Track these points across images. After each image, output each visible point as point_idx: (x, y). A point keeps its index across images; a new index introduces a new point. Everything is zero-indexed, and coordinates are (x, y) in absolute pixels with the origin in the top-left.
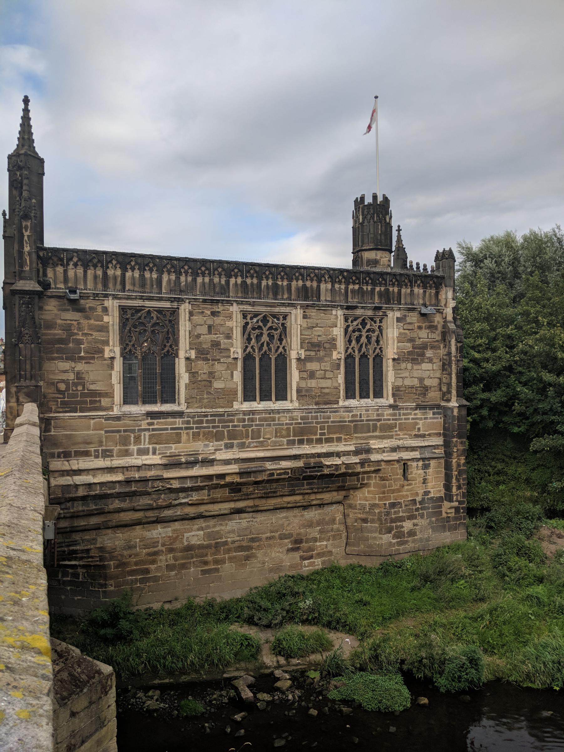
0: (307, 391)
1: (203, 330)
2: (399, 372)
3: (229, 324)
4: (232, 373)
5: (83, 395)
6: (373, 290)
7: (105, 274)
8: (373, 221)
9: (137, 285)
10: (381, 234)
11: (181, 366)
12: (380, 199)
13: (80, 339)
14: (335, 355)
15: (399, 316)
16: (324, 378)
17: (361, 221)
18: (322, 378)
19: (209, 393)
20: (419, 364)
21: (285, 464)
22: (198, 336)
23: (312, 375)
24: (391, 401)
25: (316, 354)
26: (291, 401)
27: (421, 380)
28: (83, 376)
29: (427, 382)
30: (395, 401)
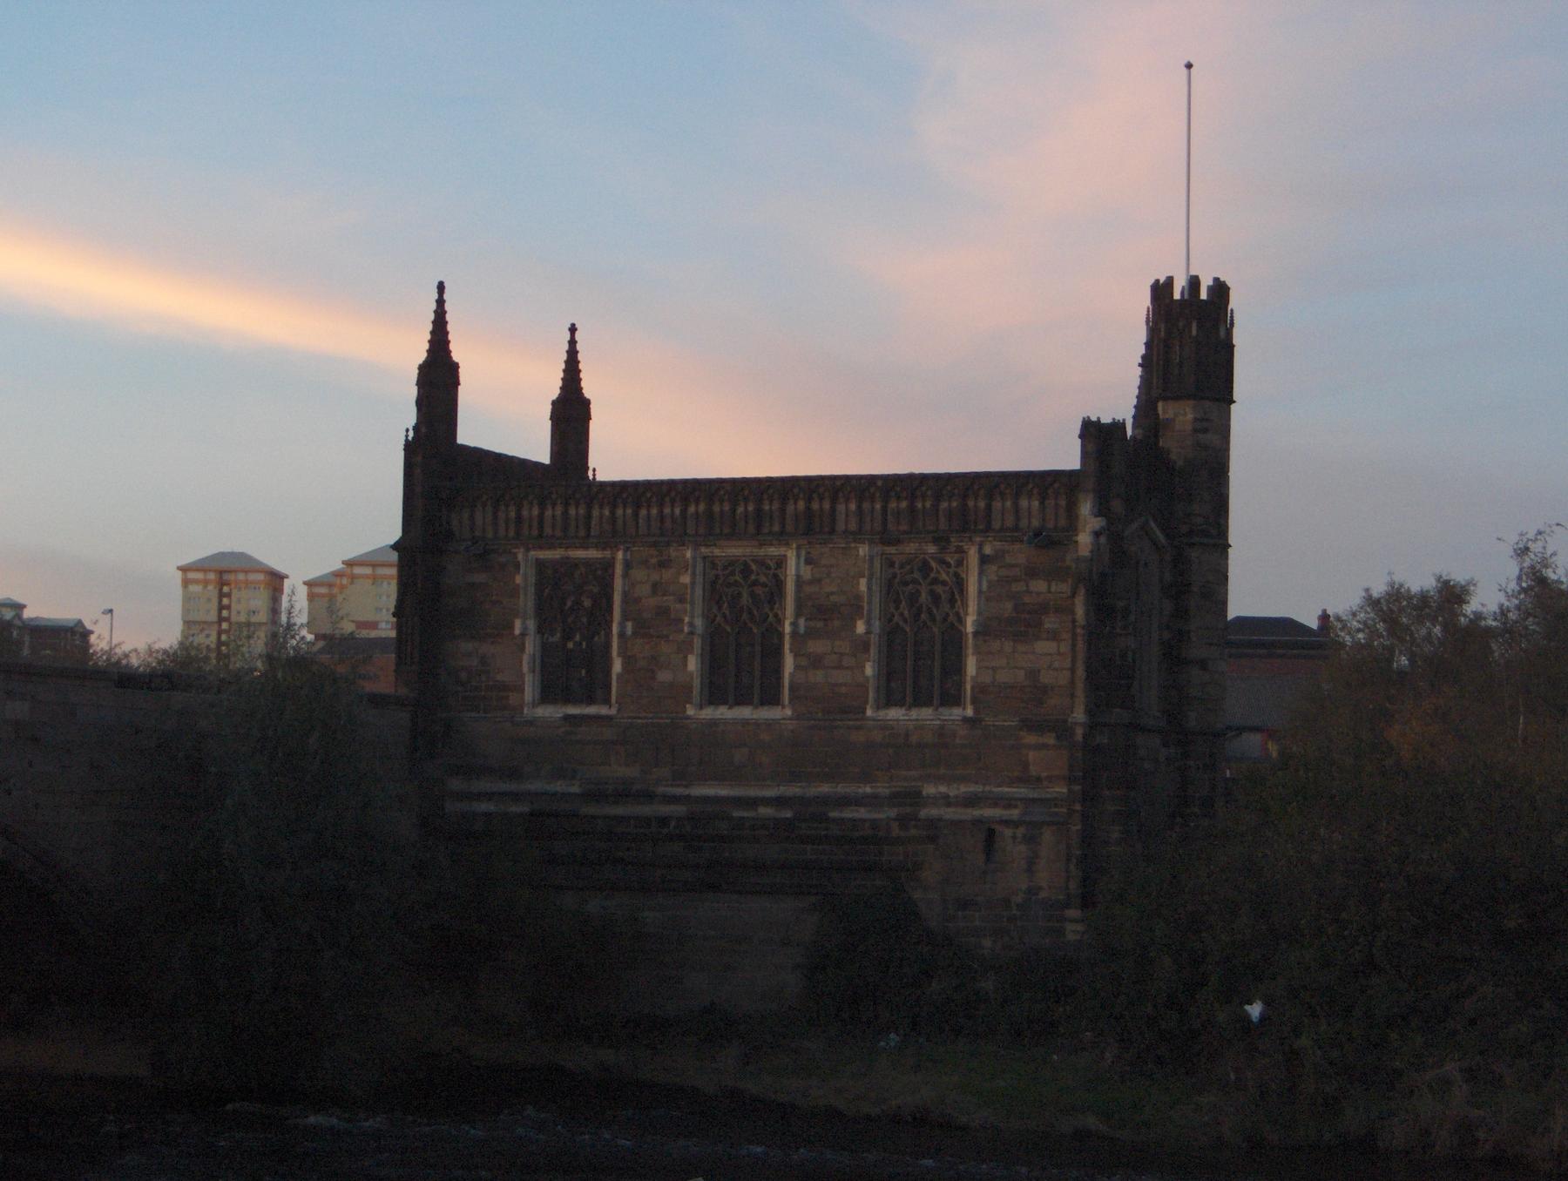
1: (643, 590)
3: (686, 579)
6: (936, 507)
10: (1181, 365)
12: (1206, 283)
14: (861, 628)
15: (988, 550)
16: (839, 667)
21: (764, 811)
23: (817, 662)
24: (969, 712)
27: (1033, 674)
29: (1046, 678)
30: (976, 711)
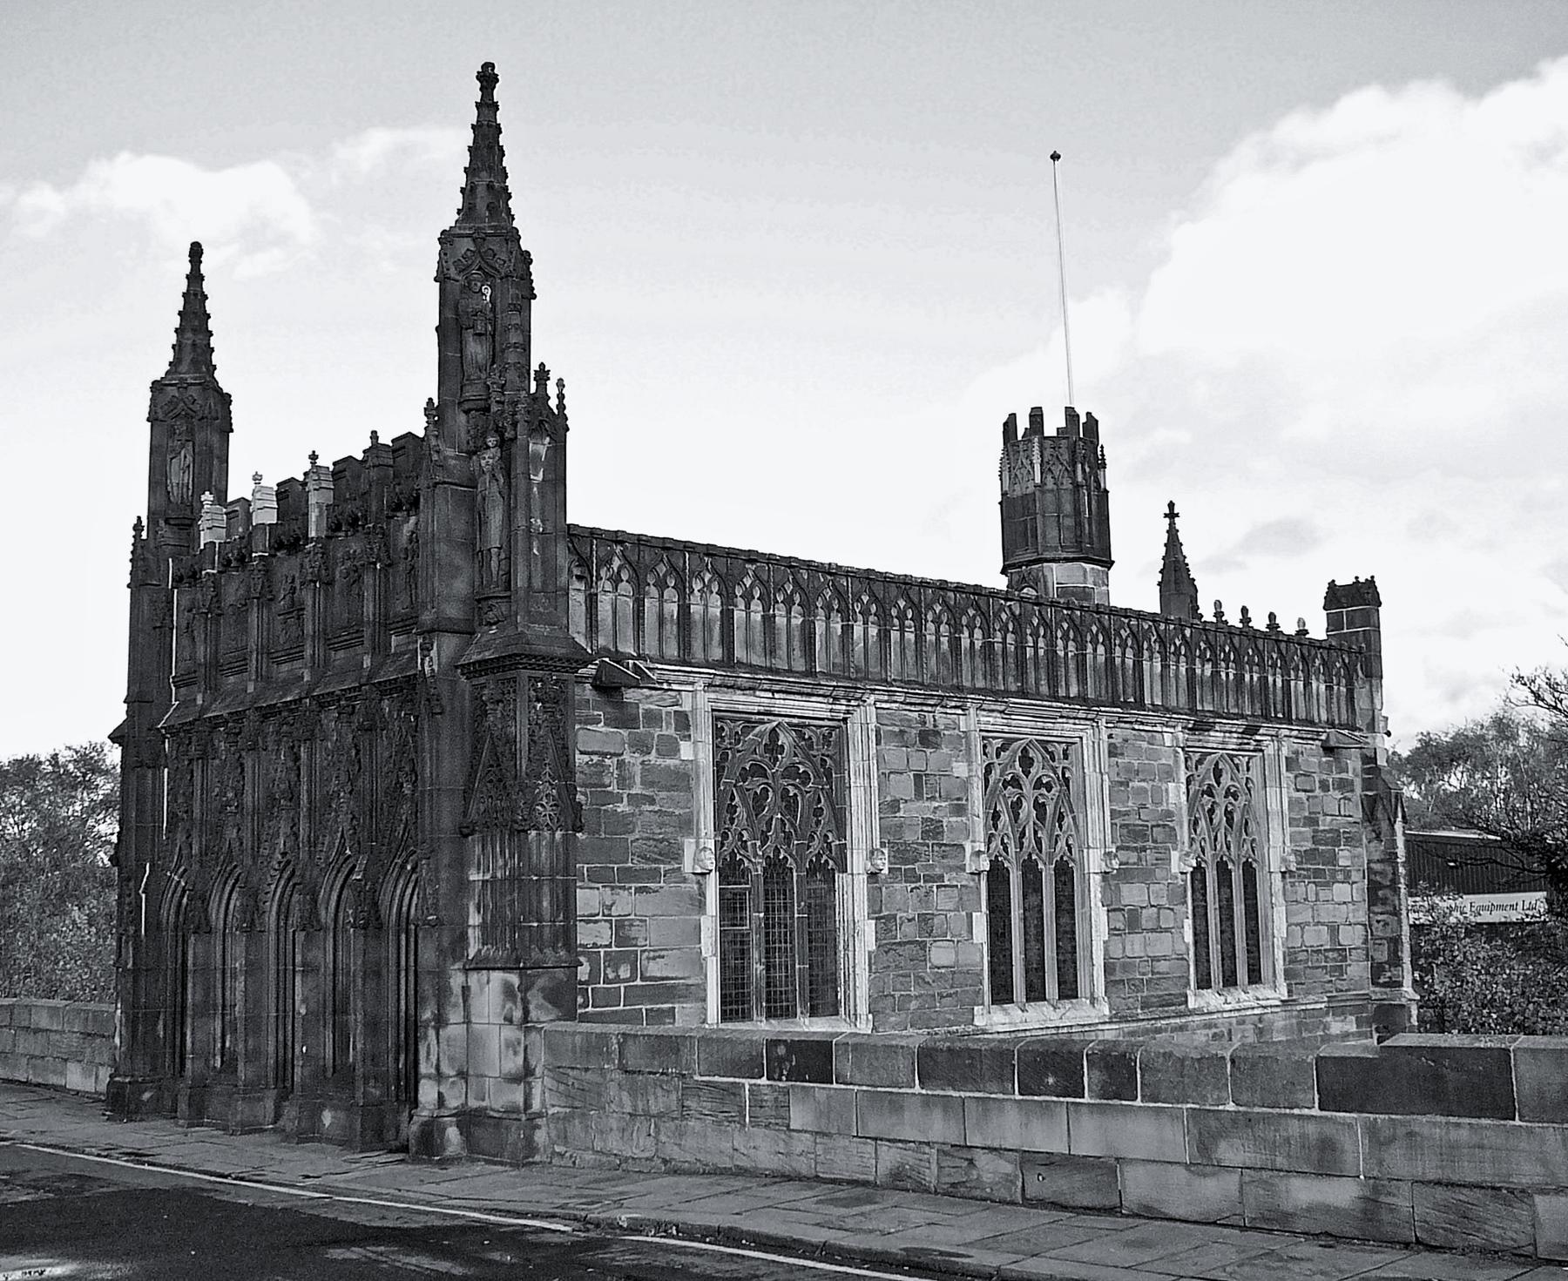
0: (1124, 966)
1: (903, 786)
2: (1295, 907)
4: (970, 916)
5: (633, 995)
7: (684, 610)
8: (1056, 480)
9: (759, 649)
11: (853, 895)
13: (624, 815)
17: (1038, 480)
18: (1153, 930)
19: (920, 981)
20: (1328, 885)
22: (894, 806)
25: (1140, 859)
26: (1093, 1000)
28: (633, 933)
